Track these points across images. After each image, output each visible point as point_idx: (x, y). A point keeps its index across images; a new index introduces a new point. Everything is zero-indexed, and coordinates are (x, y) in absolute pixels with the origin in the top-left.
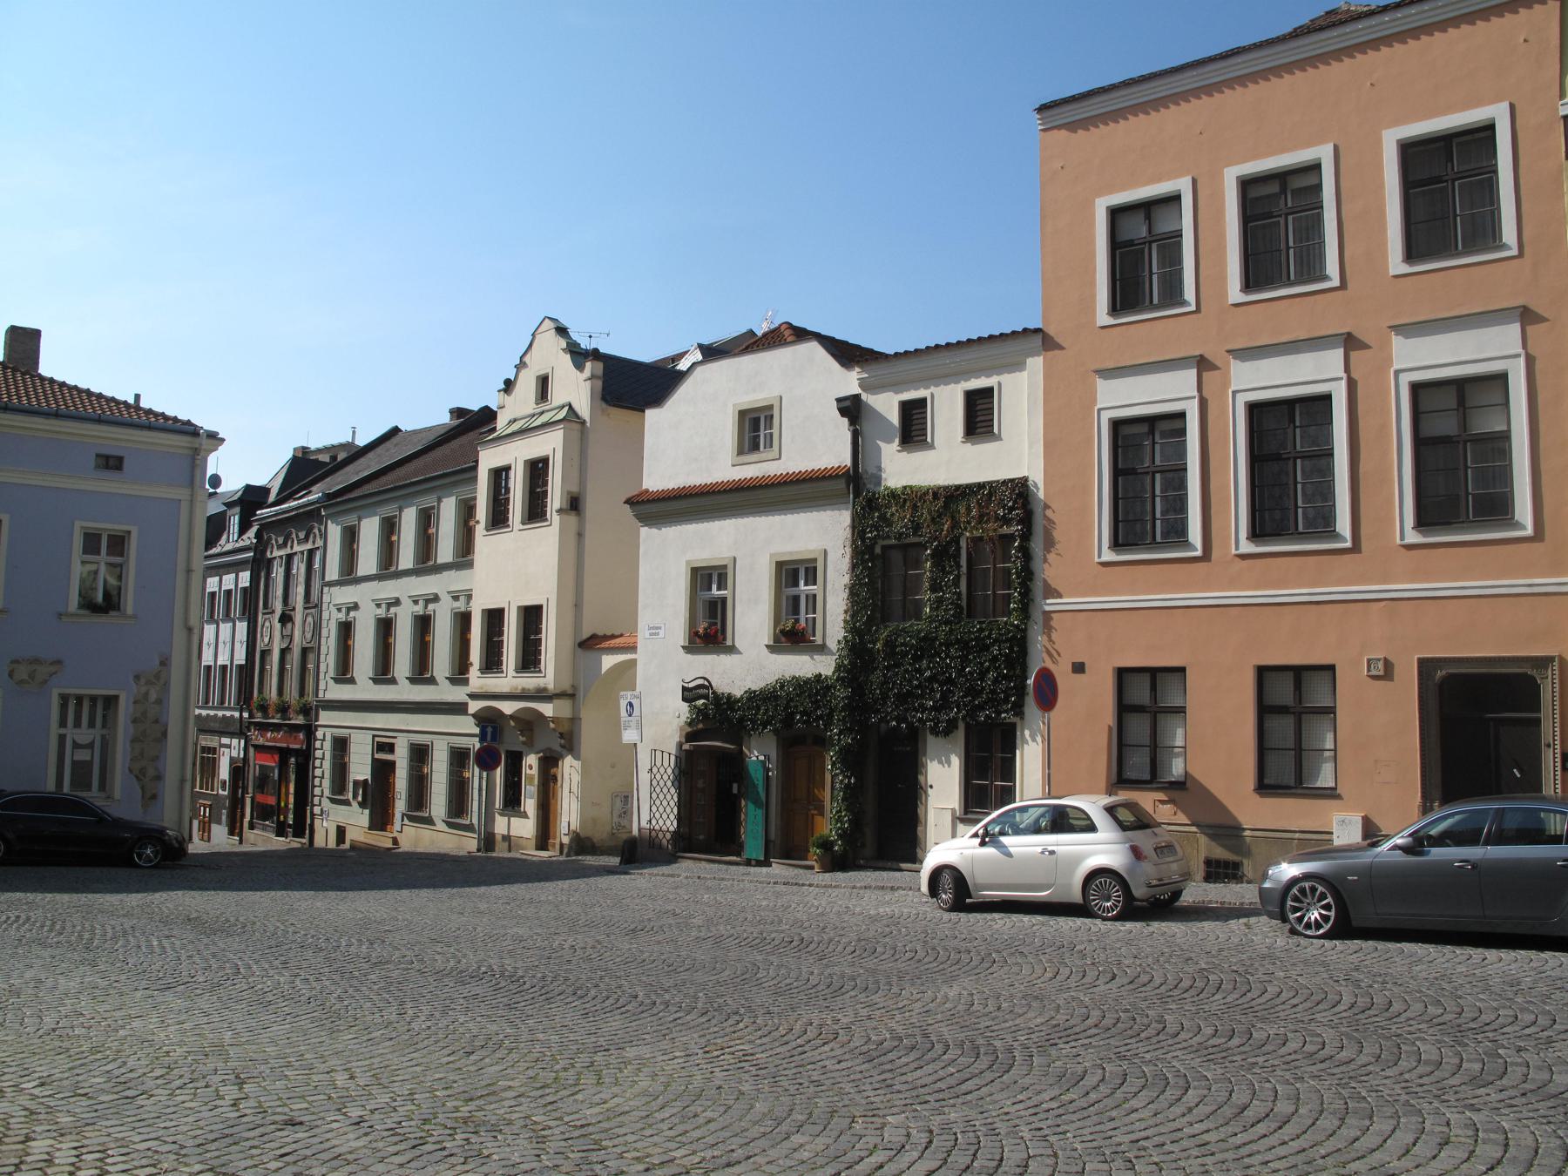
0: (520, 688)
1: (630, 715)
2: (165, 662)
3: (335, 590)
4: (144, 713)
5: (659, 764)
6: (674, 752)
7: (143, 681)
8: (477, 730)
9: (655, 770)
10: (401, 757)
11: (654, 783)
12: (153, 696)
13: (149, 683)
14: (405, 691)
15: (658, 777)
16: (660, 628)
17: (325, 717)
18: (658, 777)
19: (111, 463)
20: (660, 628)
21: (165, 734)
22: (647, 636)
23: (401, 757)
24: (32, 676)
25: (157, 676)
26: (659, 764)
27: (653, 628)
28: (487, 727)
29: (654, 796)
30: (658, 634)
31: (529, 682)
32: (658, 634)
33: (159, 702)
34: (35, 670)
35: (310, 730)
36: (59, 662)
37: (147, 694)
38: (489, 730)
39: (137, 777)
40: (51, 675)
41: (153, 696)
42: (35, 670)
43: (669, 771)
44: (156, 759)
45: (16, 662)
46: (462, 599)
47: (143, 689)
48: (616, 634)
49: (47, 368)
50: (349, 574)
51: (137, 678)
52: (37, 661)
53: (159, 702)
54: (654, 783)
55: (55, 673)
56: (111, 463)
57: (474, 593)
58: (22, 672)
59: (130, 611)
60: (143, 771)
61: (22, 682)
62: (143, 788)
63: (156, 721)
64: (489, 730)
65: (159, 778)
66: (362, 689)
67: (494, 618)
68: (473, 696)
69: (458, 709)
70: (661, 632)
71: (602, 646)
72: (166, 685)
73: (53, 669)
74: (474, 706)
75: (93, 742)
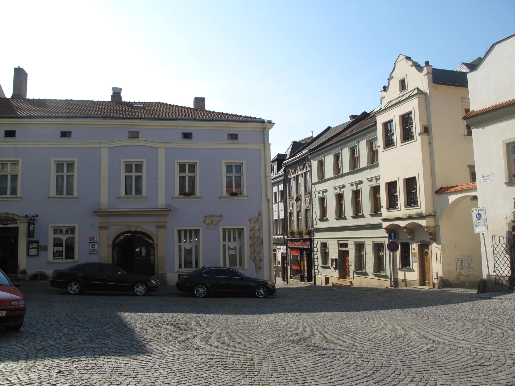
0: (408, 214)
1: (479, 219)
2: (260, 214)
3: (317, 186)
4: (254, 235)
5: (497, 242)
6: (505, 236)
7: (252, 222)
8: (387, 235)
9: (495, 246)
10: (351, 249)
11: (496, 252)
12: (257, 228)
13: (254, 222)
14: (350, 222)
15: (498, 249)
16: (490, 176)
17: (317, 235)
18: (498, 249)
19: (233, 137)
20: (490, 176)
21: (262, 243)
22: (482, 180)
23: (351, 249)
24: (212, 222)
25: (258, 220)
26: (497, 242)
27: (486, 176)
28: (392, 233)
30: (489, 179)
31: (412, 211)
32: (489, 179)
33: (259, 230)
34: (213, 220)
35: (311, 241)
36: (221, 216)
37: (254, 227)
38: (393, 234)
39: (253, 260)
40: (218, 222)
41: (257, 228)
42: (213, 220)
43: (504, 246)
44: (260, 253)
45: (206, 217)
46: (374, 181)
47: (253, 225)
48: (453, 185)
49: (207, 108)
50: (322, 178)
51: (250, 221)
52: (213, 216)
53: (259, 230)
55: (220, 220)
56: (233, 137)
57: (380, 177)
58: (208, 221)
59: (245, 194)
61: (208, 224)
62: (255, 265)
63: (259, 238)
64: (393, 234)
65: (261, 260)
66: (332, 222)
67: (392, 186)
68: (384, 220)
69: (378, 226)
70: (491, 178)
71: (448, 191)
72: (261, 223)
73: (219, 219)
74: (385, 225)
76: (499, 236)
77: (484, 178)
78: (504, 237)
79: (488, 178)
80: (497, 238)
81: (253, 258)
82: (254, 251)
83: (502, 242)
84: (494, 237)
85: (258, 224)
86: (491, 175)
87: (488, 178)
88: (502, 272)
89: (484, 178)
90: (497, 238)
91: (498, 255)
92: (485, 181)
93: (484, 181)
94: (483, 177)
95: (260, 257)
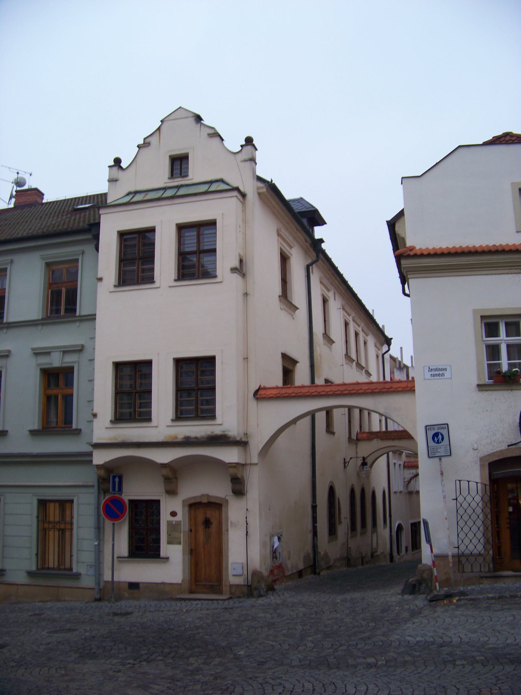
5: (465, 493)
6: (478, 480)
9: (460, 499)
11: (461, 511)
16: (445, 369)
18: (465, 505)
20: (445, 369)
22: (429, 377)
26: (465, 493)
27: (436, 370)
29: (461, 523)
30: (443, 375)
32: (443, 375)
43: (478, 499)
54: (461, 511)
70: (447, 374)
76: (469, 482)
77: (432, 373)
78: (477, 483)
79: (441, 372)
80: (464, 485)
83: (473, 492)
84: (458, 482)
86: (448, 369)
87: (441, 372)
88: (471, 547)
89: (432, 373)
90: (464, 485)
91: (466, 517)
92: (435, 378)
93: (433, 378)
94: (430, 370)
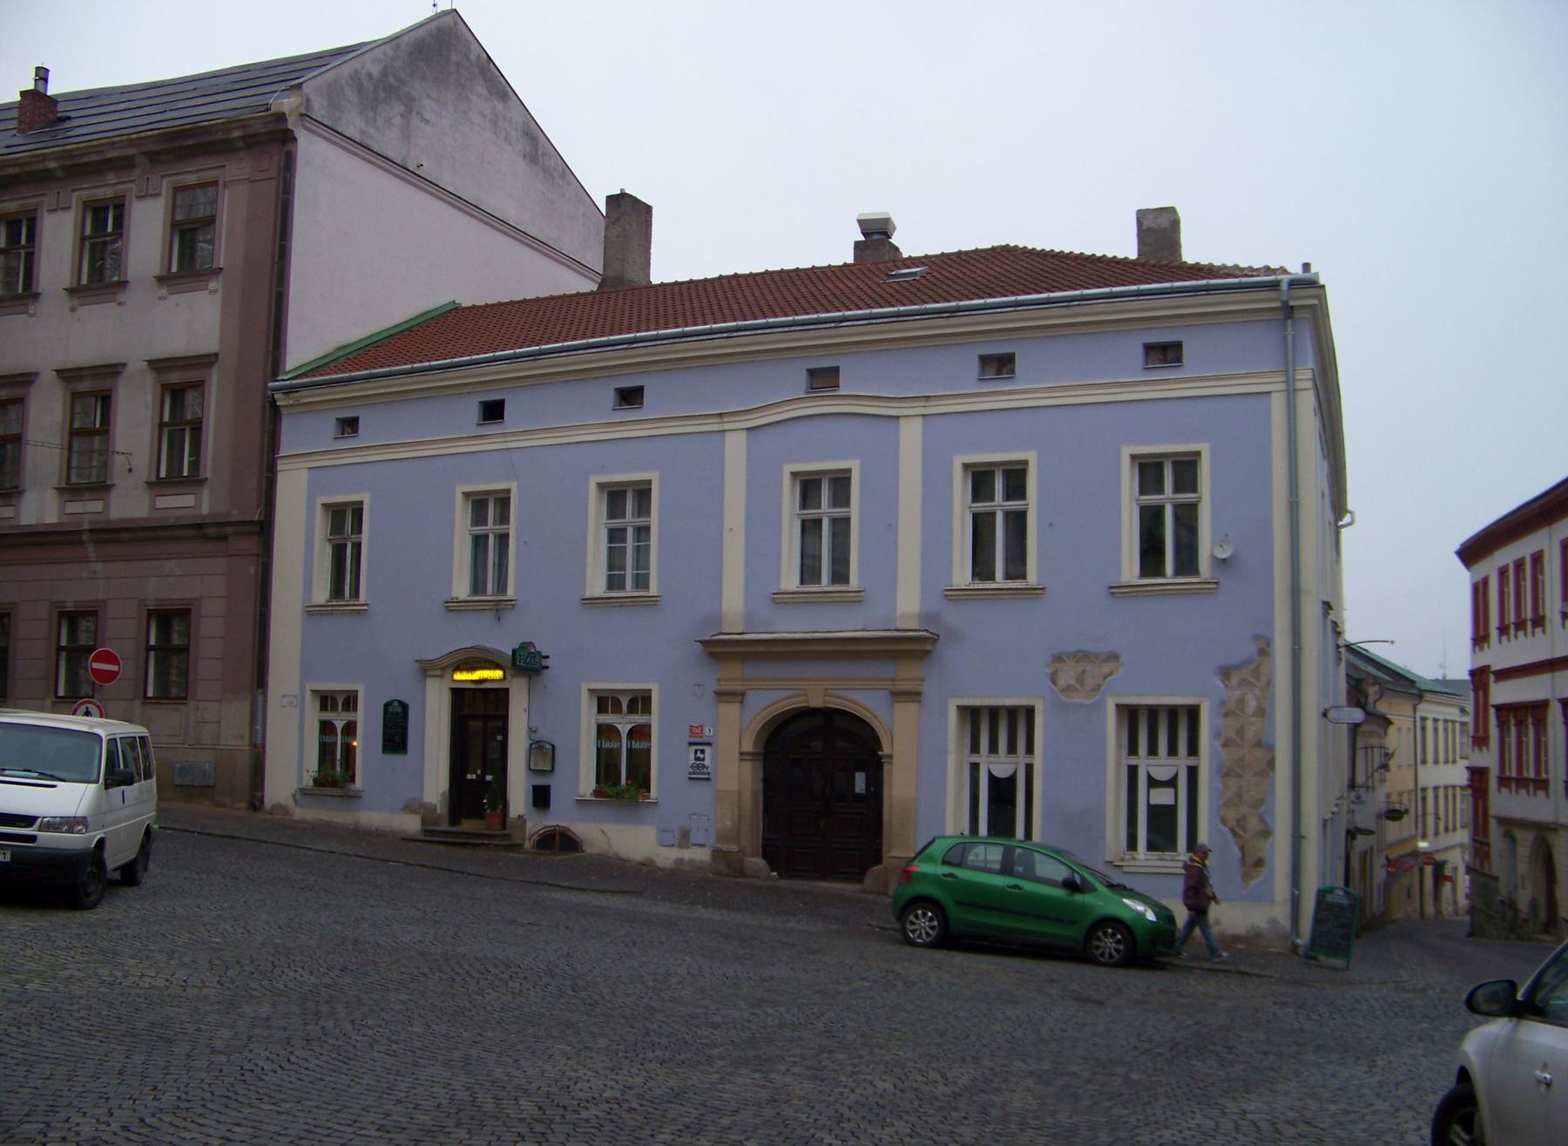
2: (1265, 651)
4: (1240, 732)
7: (1234, 681)
12: (1251, 705)
13: (1243, 683)
21: (1271, 764)
24: (1080, 678)
25: (1256, 673)
34: (1083, 672)
37: (1241, 702)
39: (1232, 830)
41: (1251, 705)
44: (1260, 802)
45: (1058, 659)
47: (1237, 694)
53: (1261, 712)
55: (1111, 674)
58: (1067, 676)
60: (1241, 821)
61: (1068, 689)
62: (1242, 849)
63: (1258, 744)
65: (1266, 833)
72: (1270, 683)
73: (1107, 668)
75: (1176, 775)
81: (1234, 823)
82: (1239, 795)
85: (1257, 691)
95: (1262, 819)
